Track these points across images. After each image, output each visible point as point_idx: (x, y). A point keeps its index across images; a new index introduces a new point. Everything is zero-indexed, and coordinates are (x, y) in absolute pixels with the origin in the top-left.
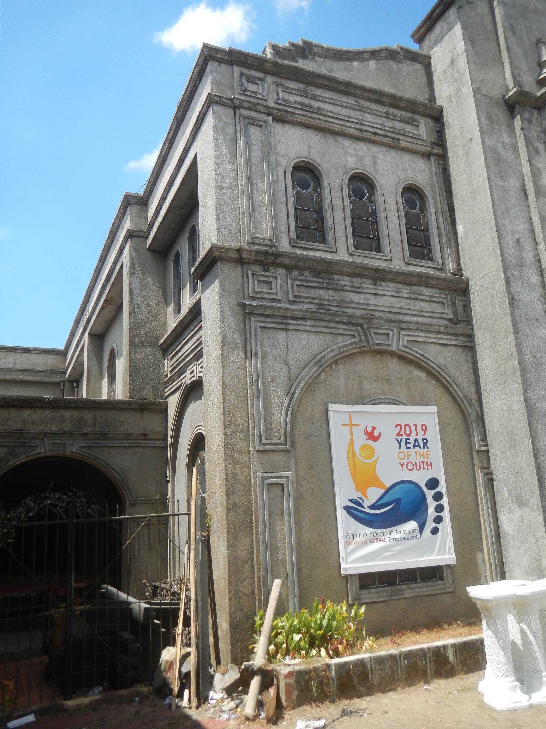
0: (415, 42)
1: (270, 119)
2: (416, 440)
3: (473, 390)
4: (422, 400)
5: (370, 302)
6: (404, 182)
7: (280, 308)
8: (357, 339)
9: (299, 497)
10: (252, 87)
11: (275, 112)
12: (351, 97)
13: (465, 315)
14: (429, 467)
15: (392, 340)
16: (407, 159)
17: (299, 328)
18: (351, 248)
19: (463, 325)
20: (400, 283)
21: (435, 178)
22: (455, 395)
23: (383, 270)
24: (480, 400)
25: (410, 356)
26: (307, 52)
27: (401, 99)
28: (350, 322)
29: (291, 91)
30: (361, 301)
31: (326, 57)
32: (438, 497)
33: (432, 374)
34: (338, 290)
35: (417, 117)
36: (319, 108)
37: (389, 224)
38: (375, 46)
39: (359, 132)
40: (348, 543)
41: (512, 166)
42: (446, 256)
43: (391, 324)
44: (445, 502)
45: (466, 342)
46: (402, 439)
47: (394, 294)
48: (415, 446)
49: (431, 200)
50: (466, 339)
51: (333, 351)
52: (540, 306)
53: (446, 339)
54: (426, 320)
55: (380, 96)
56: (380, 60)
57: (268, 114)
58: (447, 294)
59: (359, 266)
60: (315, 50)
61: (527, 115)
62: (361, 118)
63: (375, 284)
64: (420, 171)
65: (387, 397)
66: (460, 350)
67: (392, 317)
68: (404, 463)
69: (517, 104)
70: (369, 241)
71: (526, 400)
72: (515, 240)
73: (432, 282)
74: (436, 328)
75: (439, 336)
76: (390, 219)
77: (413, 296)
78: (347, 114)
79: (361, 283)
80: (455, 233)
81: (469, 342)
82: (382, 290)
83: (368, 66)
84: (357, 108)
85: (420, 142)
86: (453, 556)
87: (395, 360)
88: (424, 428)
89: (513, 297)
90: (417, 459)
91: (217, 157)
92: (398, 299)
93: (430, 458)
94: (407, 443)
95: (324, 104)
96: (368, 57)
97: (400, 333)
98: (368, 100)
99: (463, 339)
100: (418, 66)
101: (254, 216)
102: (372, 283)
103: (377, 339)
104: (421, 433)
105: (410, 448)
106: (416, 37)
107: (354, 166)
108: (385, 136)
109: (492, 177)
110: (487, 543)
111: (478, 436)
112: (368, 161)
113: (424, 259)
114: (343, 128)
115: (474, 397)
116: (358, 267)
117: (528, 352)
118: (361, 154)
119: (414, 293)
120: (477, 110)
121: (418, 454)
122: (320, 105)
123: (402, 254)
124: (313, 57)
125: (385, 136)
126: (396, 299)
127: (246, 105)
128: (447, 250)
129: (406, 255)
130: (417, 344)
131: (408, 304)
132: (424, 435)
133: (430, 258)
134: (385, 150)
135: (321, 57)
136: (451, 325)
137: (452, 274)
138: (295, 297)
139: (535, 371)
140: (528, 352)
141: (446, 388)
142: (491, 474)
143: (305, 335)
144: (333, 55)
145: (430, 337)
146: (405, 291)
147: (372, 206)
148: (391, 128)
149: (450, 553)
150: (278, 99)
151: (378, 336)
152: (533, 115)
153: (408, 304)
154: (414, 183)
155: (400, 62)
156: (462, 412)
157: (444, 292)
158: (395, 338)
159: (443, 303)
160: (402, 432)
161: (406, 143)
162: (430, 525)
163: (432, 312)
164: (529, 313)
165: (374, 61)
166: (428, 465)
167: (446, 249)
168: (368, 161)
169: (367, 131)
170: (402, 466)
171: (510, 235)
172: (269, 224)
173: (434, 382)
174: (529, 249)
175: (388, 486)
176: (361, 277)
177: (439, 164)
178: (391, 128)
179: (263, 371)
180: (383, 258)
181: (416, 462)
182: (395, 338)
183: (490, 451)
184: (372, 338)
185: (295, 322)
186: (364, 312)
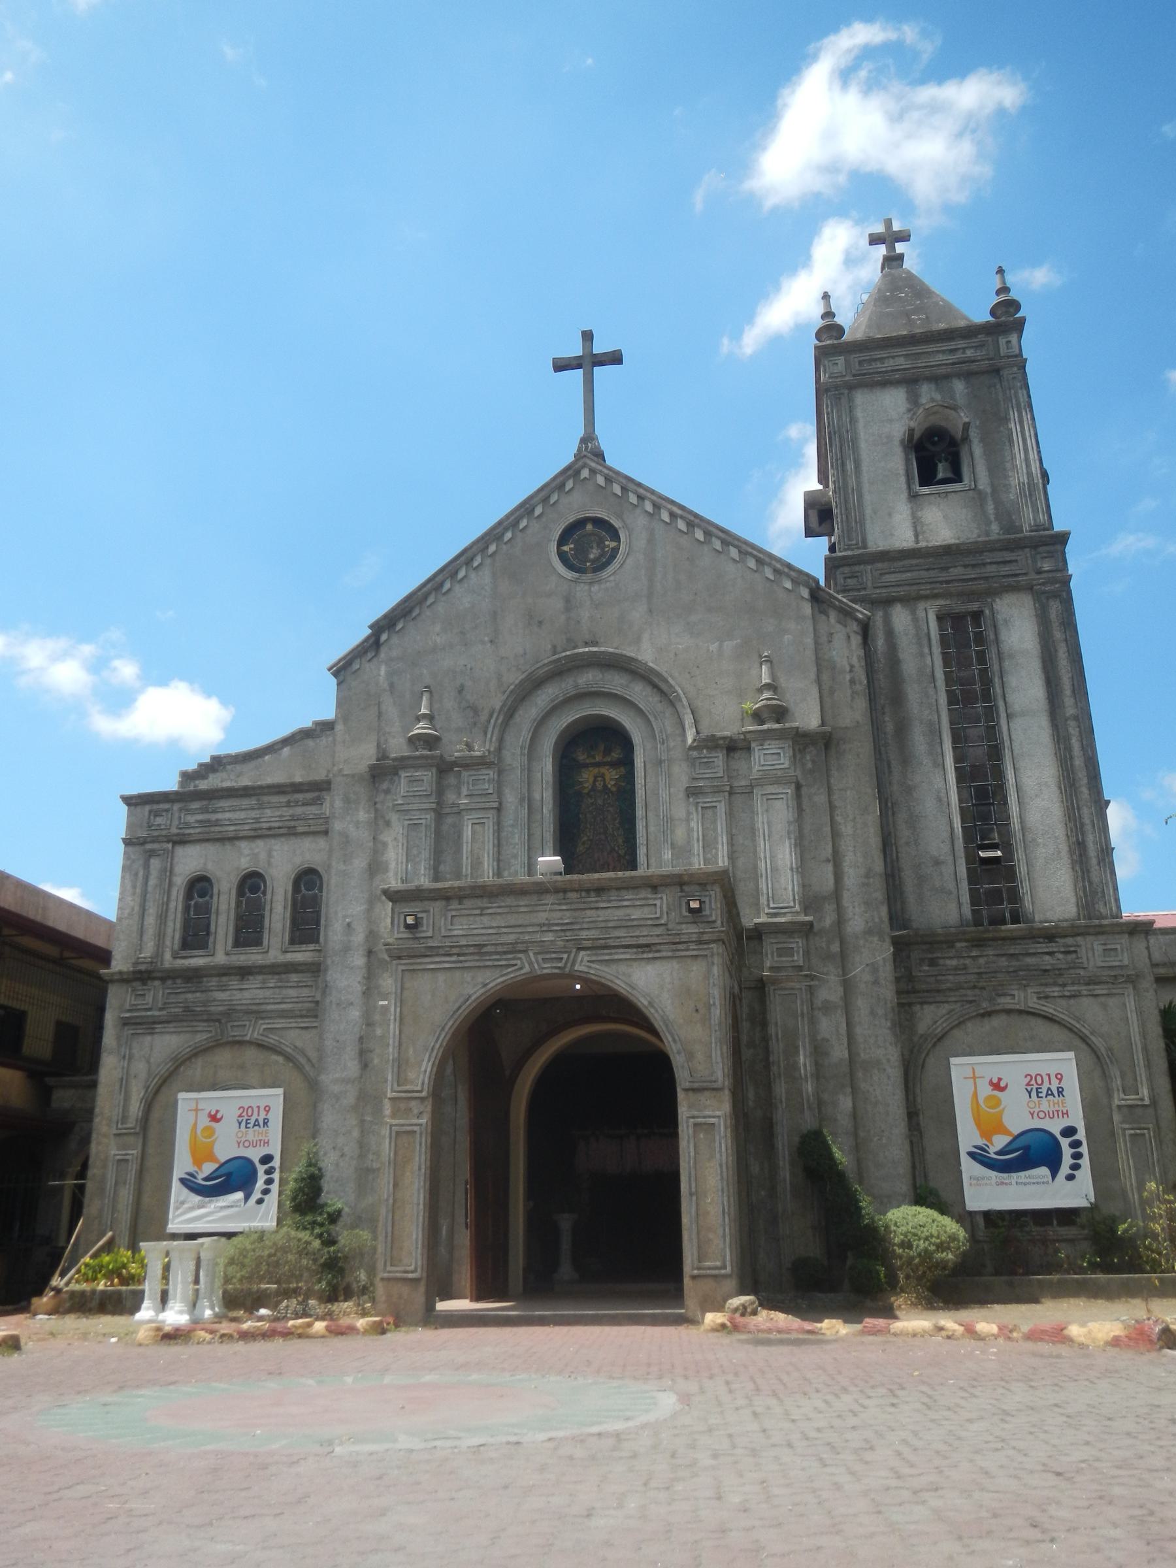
1: (170, 846)
7: (148, 1016)
8: (213, 1033)
10: (159, 820)
11: (175, 838)
12: (253, 798)
18: (229, 948)
20: (270, 974)
27: (301, 784)
28: (211, 1019)
29: (193, 812)
32: (269, 1172)
33: (288, 1058)
34: (205, 991)
36: (217, 820)
40: (177, 1208)
47: (258, 986)
48: (255, 1125)
51: (190, 1047)
54: (290, 1006)
57: (168, 842)
59: (223, 967)
60: (225, 761)
61: (385, 786)
67: (254, 1008)
74: (298, 1013)
76: (274, 911)
77: (279, 984)
85: (321, 821)
91: (121, 893)
94: (247, 1123)
101: (141, 940)
107: (247, 866)
108: (279, 828)
112: (263, 856)
118: (256, 851)
122: (220, 816)
124: (224, 768)
127: (149, 840)
133: (317, 941)
138: (165, 1003)
143: (167, 1037)
150: (180, 823)
151: (235, 1029)
155: (318, 737)
160: (245, 1114)
162: (257, 1195)
165: (288, 748)
168: (263, 856)
169: (261, 829)
170: (239, 1143)
172: (152, 943)
173: (291, 1065)
175: (223, 1160)
186: (226, 1008)
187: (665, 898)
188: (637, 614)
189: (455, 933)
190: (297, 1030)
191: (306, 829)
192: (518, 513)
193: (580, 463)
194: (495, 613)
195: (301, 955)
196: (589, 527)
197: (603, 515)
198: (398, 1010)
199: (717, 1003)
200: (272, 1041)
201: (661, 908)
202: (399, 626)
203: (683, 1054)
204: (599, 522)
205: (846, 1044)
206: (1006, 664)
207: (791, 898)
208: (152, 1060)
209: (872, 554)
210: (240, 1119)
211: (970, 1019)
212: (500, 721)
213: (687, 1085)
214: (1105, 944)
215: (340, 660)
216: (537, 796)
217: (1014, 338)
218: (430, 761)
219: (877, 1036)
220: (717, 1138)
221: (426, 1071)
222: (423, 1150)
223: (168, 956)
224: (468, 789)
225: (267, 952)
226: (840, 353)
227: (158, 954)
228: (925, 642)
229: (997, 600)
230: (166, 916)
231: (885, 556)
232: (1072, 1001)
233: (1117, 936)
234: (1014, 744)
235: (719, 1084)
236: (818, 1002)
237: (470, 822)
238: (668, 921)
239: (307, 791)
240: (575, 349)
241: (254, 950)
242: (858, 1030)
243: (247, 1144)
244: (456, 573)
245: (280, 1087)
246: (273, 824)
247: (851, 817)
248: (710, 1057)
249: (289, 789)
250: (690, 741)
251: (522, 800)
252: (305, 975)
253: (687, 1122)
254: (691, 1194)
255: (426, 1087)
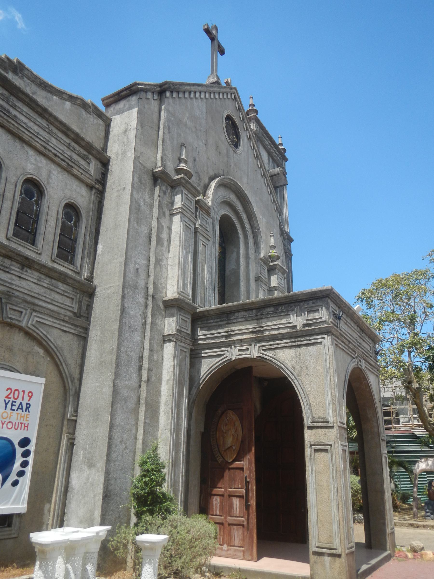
0: (103, 104)
2: (21, 404)
3: (77, 371)
4: (35, 371)
5: (13, 282)
6: (68, 199)
12: (44, 120)
13: (86, 312)
14: (26, 428)
15: (24, 317)
16: (75, 184)
18: (10, 234)
19: (83, 319)
21: (92, 205)
22: (63, 372)
23: (32, 260)
24: (80, 380)
25: (35, 334)
26: (18, 70)
27: (82, 139)
30: (6, 280)
31: (33, 81)
32: (26, 454)
33: (48, 352)
35: (90, 157)
36: (15, 116)
37: (47, 226)
38: (75, 94)
39: (43, 148)
41: (146, 218)
42: (84, 265)
43: (26, 305)
44: (31, 459)
45: (82, 332)
46: (9, 401)
47: (35, 281)
48: (18, 408)
49: (84, 219)
50: (82, 331)
52: (140, 320)
53: (67, 327)
54: (56, 309)
55: (68, 130)
56: (75, 104)
58: (78, 293)
59: (13, 251)
60: (26, 72)
62: (48, 139)
63: (22, 269)
64: (82, 196)
65: (5, 363)
66: (76, 338)
67: (29, 299)
68: (5, 422)
69: (160, 178)
70: (27, 234)
71: (114, 386)
72: (135, 268)
73: (69, 281)
74: (62, 317)
75: (62, 324)
76: (49, 223)
78: (38, 131)
79: (11, 265)
80: (96, 250)
81: (84, 333)
82: (27, 275)
83: (64, 104)
84: (47, 130)
85: (88, 176)
86: (26, 506)
87: (21, 334)
88: (30, 394)
89: (124, 309)
90: (17, 420)
92: (38, 287)
93: (28, 421)
94: (12, 405)
95: (21, 115)
96: (66, 98)
97: (32, 313)
98: (57, 128)
99: (80, 330)
100: (101, 122)
102: (20, 267)
103: (11, 314)
104: (26, 398)
105: (14, 410)
106: (105, 102)
107: (31, 171)
108: (63, 160)
109: (132, 220)
110: (55, 497)
111: (72, 408)
112: (44, 173)
113: (66, 260)
114: (31, 140)
115: (77, 376)
116: (11, 251)
117: (124, 351)
118: (40, 165)
119: (52, 285)
120: (133, 171)
121: (19, 416)
122: (17, 114)
123: (51, 252)
124: (22, 77)
125: (63, 160)
126: (36, 285)
128: (86, 260)
129: (54, 254)
130: (43, 325)
131: (45, 293)
132: (29, 401)
133: (72, 262)
134: (60, 171)
135: (29, 79)
136: (74, 317)
137: (85, 279)
139: (125, 365)
140: (124, 351)
141: (57, 365)
142: (74, 439)
144: (39, 83)
145: (55, 323)
146: (45, 281)
147: (37, 208)
148: (69, 156)
149: (23, 503)
151: (12, 312)
152: (167, 190)
153: (45, 293)
154: (75, 203)
155: (89, 113)
156: (65, 386)
157: (75, 291)
158: (26, 317)
159: (73, 299)
160: (11, 396)
161: (77, 172)
162: (13, 477)
163: (62, 304)
164: (132, 323)
166: (25, 426)
167: (85, 259)
168: (44, 173)
169: (49, 151)
171: (133, 265)
173: (48, 359)
174: (143, 278)
176: (12, 260)
177: (97, 196)
178: (69, 156)
180: (34, 250)
181: (15, 423)
182: (26, 317)
183: (78, 421)
184: (7, 312)
186: (5, 289)
188: (245, 180)
194: (206, 131)
210: (7, 400)
215: (145, 85)
218: (196, 193)
224: (201, 223)
225: (40, 254)
237: (202, 242)
239: (82, 147)
243: (10, 426)
245: (38, 376)
249: (72, 136)
250: (262, 256)
252: (68, 287)
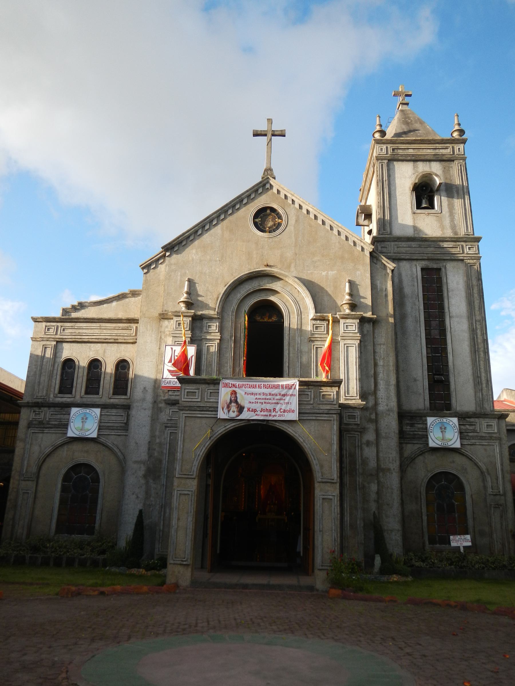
9: (35, 497)
11: (57, 340)
17: (48, 432)
75: (116, 431)
118: (98, 349)
138: (50, 419)
157: (125, 410)
168: (101, 352)
179: (30, 449)
185: (47, 429)
187: (313, 392)
189: (211, 400)
190: (115, 436)
191: (123, 341)
192: (236, 201)
193: (266, 181)
195: (118, 400)
196: (268, 211)
197: (275, 206)
198: (183, 436)
199: (335, 443)
200: (102, 441)
201: (311, 396)
202: (175, 249)
203: (318, 465)
204: (273, 210)
205: (376, 460)
206: (450, 294)
207: (355, 392)
208: (42, 446)
209: (394, 238)
211: (426, 452)
212: (223, 299)
213: (320, 480)
214: (488, 423)
216: (238, 335)
217: (461, 146)
219: (389, 458)
220: (333, 506)
221: (195, 465)
222: (193, 504)
223: (52, 396)
226: (384, 143)
227: (47, 394)
228: (416, 280)
229: (448, 264)
230: (52, 377)
231: (399, 239)
232: (472, 447)
233: (492, 419)
234: (452, 329)
235: (335, 481)
236: (364, 440)
238: (314, 402)
240: (263, 127)
241: (95, 396)
242: (381, 455)
244: (205, 226)
246: (107, 337)
247: (382, 357)
248: (331, 467)
251: (231, 337)
252: (120, 410)
253: (319, 498)
254: (320, 531)
255: (195, 473)
